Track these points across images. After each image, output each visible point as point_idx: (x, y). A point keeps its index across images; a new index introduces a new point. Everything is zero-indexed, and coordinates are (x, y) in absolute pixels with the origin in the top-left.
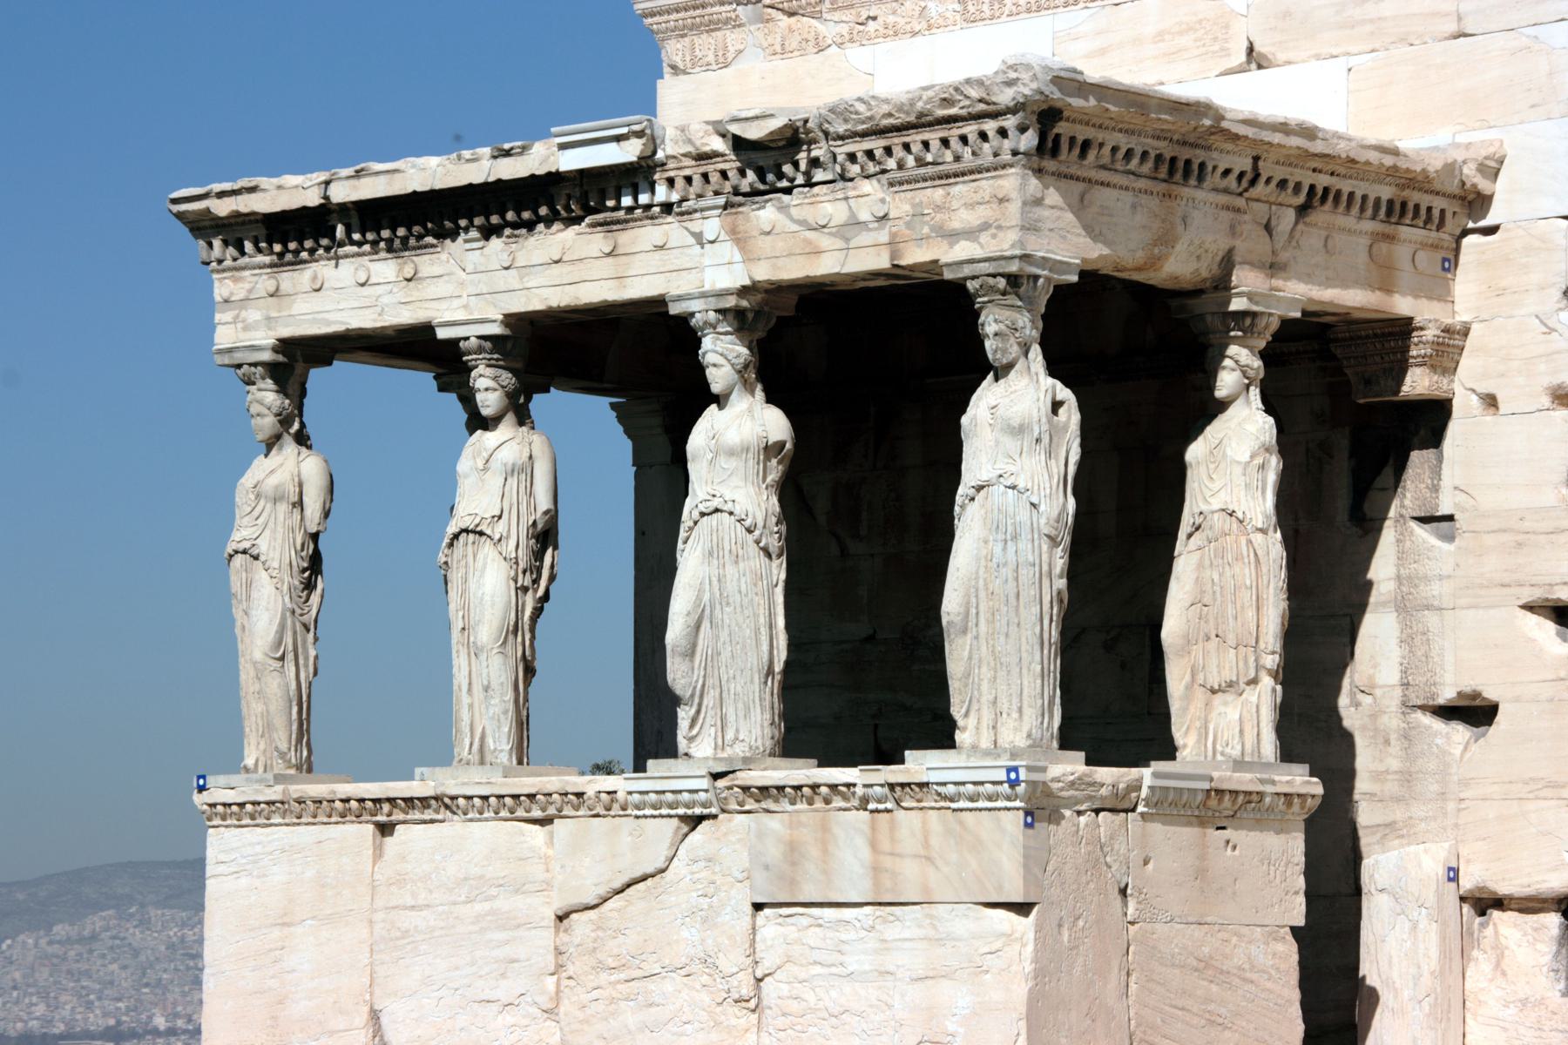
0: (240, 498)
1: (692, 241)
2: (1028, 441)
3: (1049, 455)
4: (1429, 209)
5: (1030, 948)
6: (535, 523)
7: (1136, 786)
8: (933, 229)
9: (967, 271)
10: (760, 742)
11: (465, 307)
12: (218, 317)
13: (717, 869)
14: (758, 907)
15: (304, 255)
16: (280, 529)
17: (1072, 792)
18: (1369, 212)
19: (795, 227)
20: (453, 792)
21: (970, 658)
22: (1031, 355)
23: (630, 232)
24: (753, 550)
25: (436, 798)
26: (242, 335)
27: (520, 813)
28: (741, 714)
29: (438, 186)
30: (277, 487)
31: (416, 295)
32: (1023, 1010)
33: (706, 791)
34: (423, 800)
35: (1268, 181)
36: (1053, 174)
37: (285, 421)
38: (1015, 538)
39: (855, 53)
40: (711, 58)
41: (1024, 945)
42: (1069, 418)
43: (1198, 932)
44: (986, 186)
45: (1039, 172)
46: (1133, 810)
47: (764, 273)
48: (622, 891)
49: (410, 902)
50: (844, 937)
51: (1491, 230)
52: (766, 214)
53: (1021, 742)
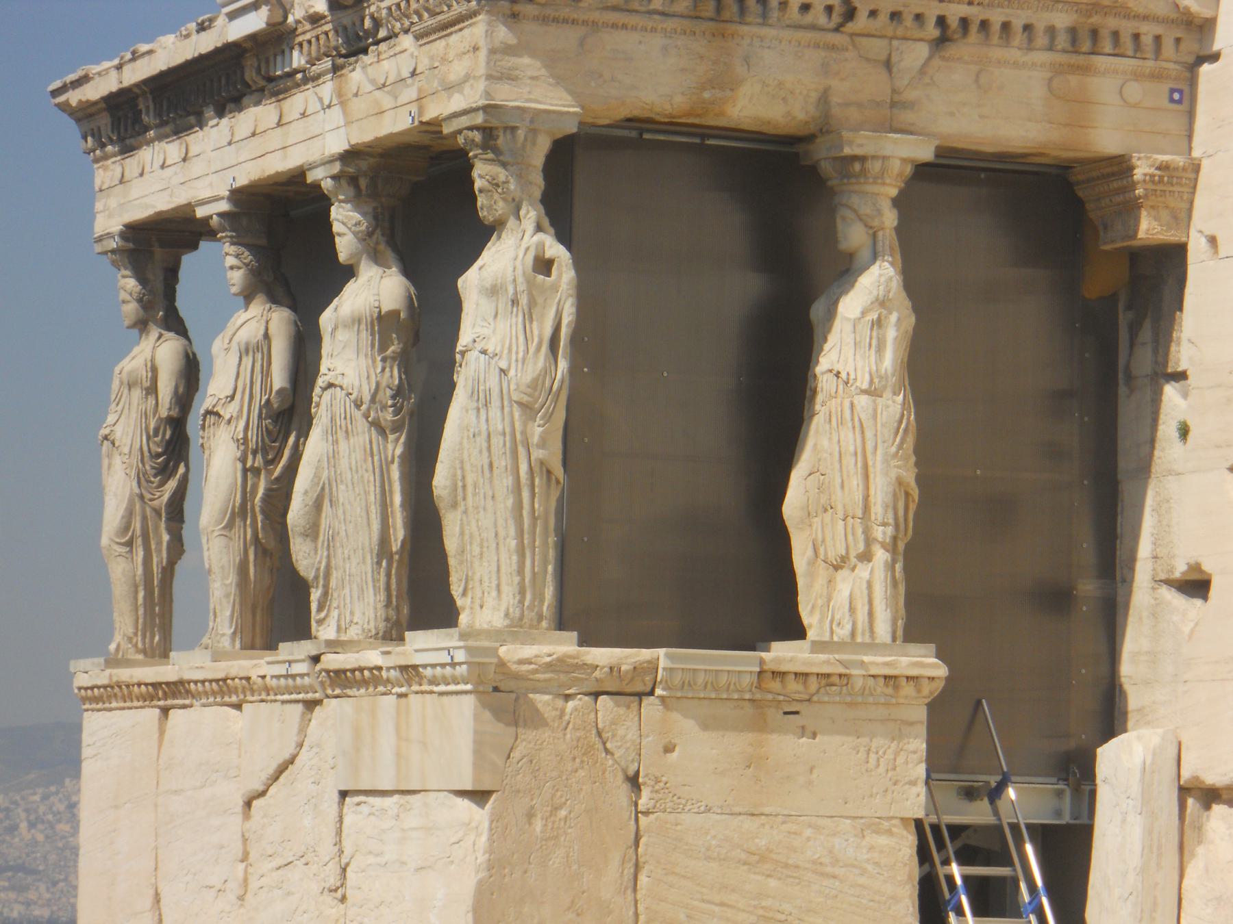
0: (115, 385)
1: (318, 107)
2: (504, 302)
3: (529, 316)
4: (1136, 36)
5: (484, 838)
6: (268, 401)
7: (653, 666)
10: (372, 625)
11: (211, 184)
14: (344, 794)
16: (134, 415)
17: (547, 676)
18: (1041, 40)
19: (369, 88)
21: (462, 533)
22: (522, 213)
24: (361, 424)
25: (181, 682)
27: (227, 699)
28: (355, 595)
29: (173, 64)
30: (129, 373)
32: (469, 901)
33: (308, 675)
35: (873, 13)
36: (536, 18)
37: (146, 304)
38: (486, 405)
41: (479, 835)
42: (560, 276)
43: (749, 824)
45: (514, 16)
46: (652, 693)
48: (277, 779)
51: (1215, 57)
52: (357, 75)
53: (498, 621)
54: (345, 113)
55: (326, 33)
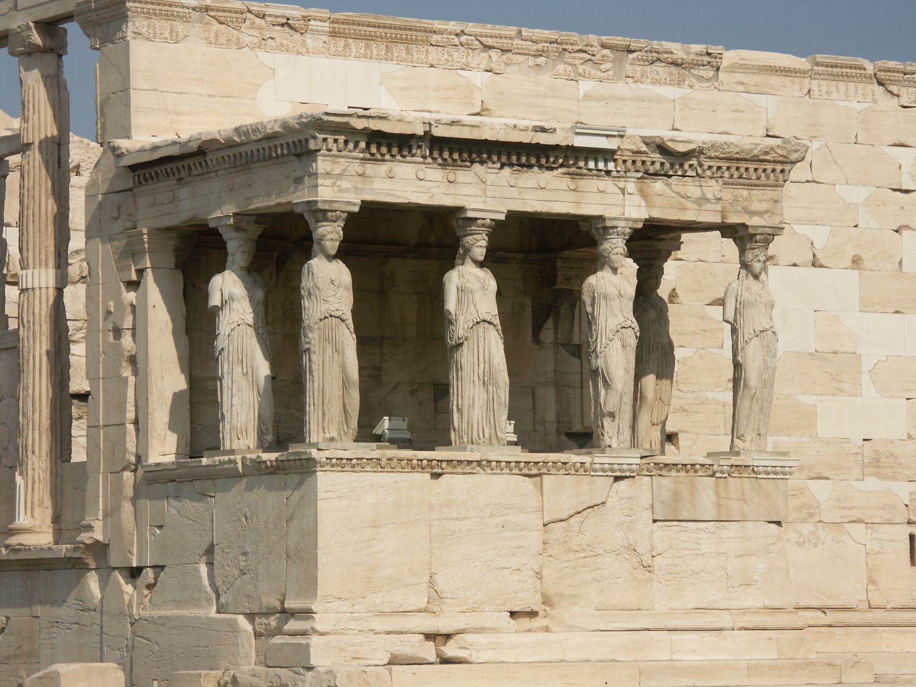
1: (619, 192)
8: (743, 208)
9: (760, 231)
12: (320, 181)
13: (634, 503)
15: (379, 157)
19: (674, 195)
20: (490, 458)
23: (584, 181)
26: (338, 194)
31: (453, 191)
34: (470, 462)
39: (261, 54)
40: (167, 35)
44: (769, 193)
47: (656, 214)
49: (455, 516)
50: (700, 536)
52: (658, 185)
54: (645, 200)
55: (643, 162)
